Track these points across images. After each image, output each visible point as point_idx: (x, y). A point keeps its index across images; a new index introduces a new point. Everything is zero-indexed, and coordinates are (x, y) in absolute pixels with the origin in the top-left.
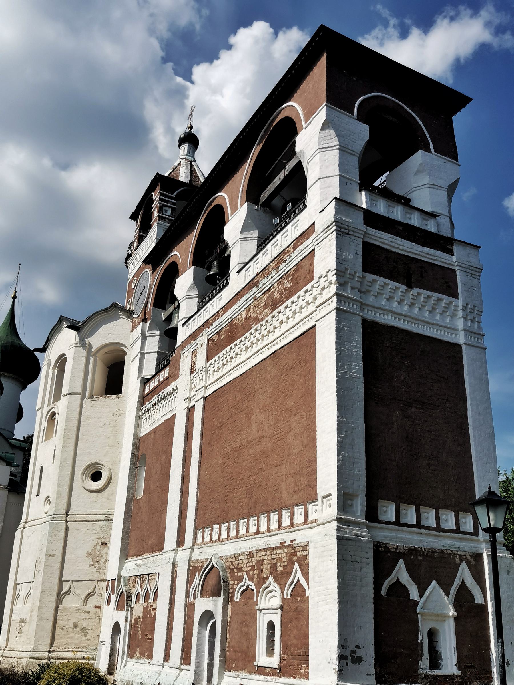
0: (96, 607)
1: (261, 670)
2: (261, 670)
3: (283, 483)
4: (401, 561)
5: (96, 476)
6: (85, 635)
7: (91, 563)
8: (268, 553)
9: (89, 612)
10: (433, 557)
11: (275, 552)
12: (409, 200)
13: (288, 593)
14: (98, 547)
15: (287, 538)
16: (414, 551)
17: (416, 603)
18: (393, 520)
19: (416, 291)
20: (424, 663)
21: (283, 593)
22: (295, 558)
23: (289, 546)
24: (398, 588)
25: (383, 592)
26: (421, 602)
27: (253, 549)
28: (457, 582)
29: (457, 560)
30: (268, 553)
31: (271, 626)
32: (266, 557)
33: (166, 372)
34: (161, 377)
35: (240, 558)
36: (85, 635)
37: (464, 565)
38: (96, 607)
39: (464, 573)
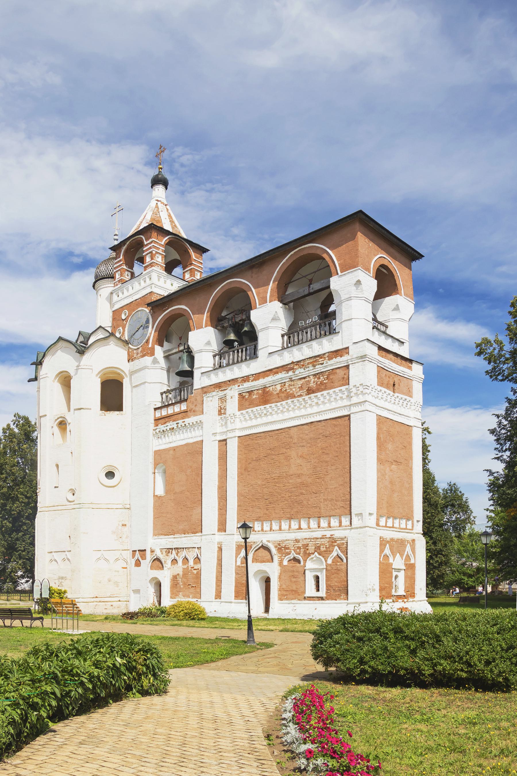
0: (123, 568)
1: (310, 598)
2: (310, 598)
3: (321, 504)
4: (388, 545)
5: (110, 475)
6: (118, 587)
7: (116, 538)
8: (312, 540)
9: (118, 571)
10: (398, 542)
11: (318, 540)
12: (387, 327)
13: (330, 561)
14: (120, 527)
15: (328, 534)
16: (392, 540)
17: (392, 564)
18: (384, 525)
19: (396, 395)
20: (393, 590)
21: (326, 561)
22: (336, 544)
23: (329, 538)
24: (386, 557)
25: (381, 560)
26: (394, 563)
27: (299, 538)
28: (406, 553)
29: (406, 543)
30: (312, 540)
31: (317, 578)
32: (311, 543)
33: (184, 407)
34: (177, 409)
35: (287, 542)
36: (118, 587)
37: (409, 545)
38: (123, 568)
39: (408, 549)
